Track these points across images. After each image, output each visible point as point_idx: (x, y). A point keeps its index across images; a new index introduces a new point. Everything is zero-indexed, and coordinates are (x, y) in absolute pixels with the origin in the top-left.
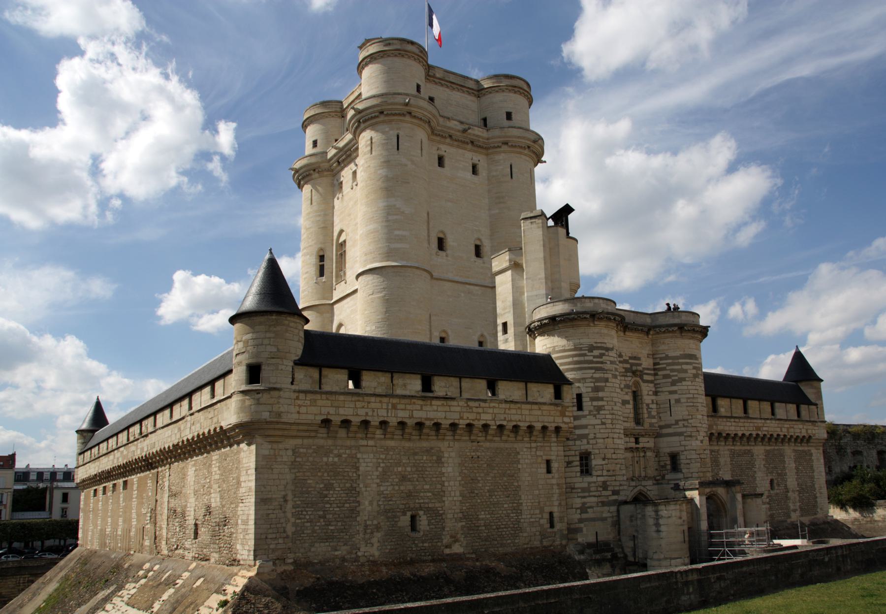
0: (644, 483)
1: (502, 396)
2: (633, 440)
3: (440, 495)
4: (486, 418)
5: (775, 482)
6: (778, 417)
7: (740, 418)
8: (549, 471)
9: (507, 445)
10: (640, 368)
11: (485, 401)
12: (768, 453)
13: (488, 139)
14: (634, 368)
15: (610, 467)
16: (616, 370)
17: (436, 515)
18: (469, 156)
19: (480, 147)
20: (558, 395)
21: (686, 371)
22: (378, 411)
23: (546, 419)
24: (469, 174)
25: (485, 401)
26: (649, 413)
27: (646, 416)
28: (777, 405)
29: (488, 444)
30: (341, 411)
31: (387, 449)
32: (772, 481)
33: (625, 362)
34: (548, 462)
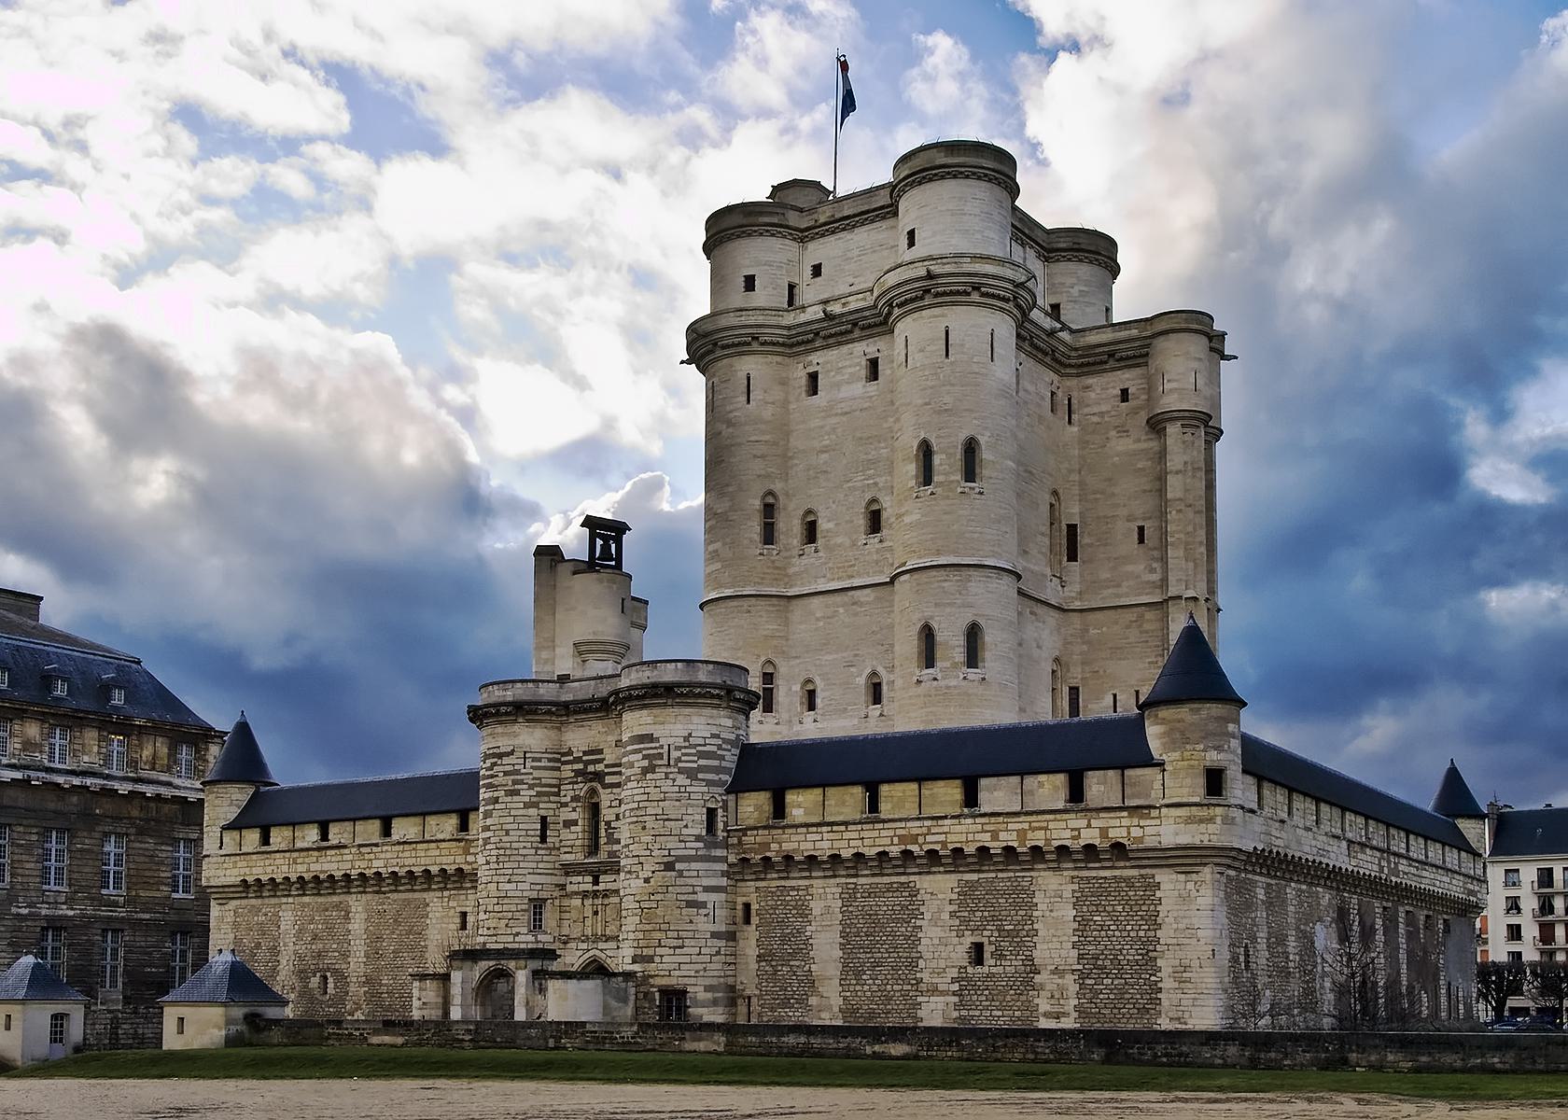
0: (601, 946)
1: (395, 837)
2: (589, 879)
3: (345, 956)
4: (378, 865)
5: (988, 949)
6: (984, 809)
7: (846, 824)
8: (464, 927)
9: (417, 895)
10: (600, 767)
11: (376, 845)
12: (966, 892)
13: (875, 306)
14: (591, 768)
15: (492, 923)
16: (514, 782)
17: (341, 977)
18: (860, 351)
19: (870, 326)
20: (464, 827)
21: (631, 765)
22: (280, 868)
23: (445, 860)
24: (860, 388)
25: (376, 845)
26: (610, 836)
27: (603, 840)
28: (983, 782)
29: (395, 896)
30: (254, 871)
31: (304, 905)
32: (978, 948)
33: (578, 760)
34: (464, 915)
